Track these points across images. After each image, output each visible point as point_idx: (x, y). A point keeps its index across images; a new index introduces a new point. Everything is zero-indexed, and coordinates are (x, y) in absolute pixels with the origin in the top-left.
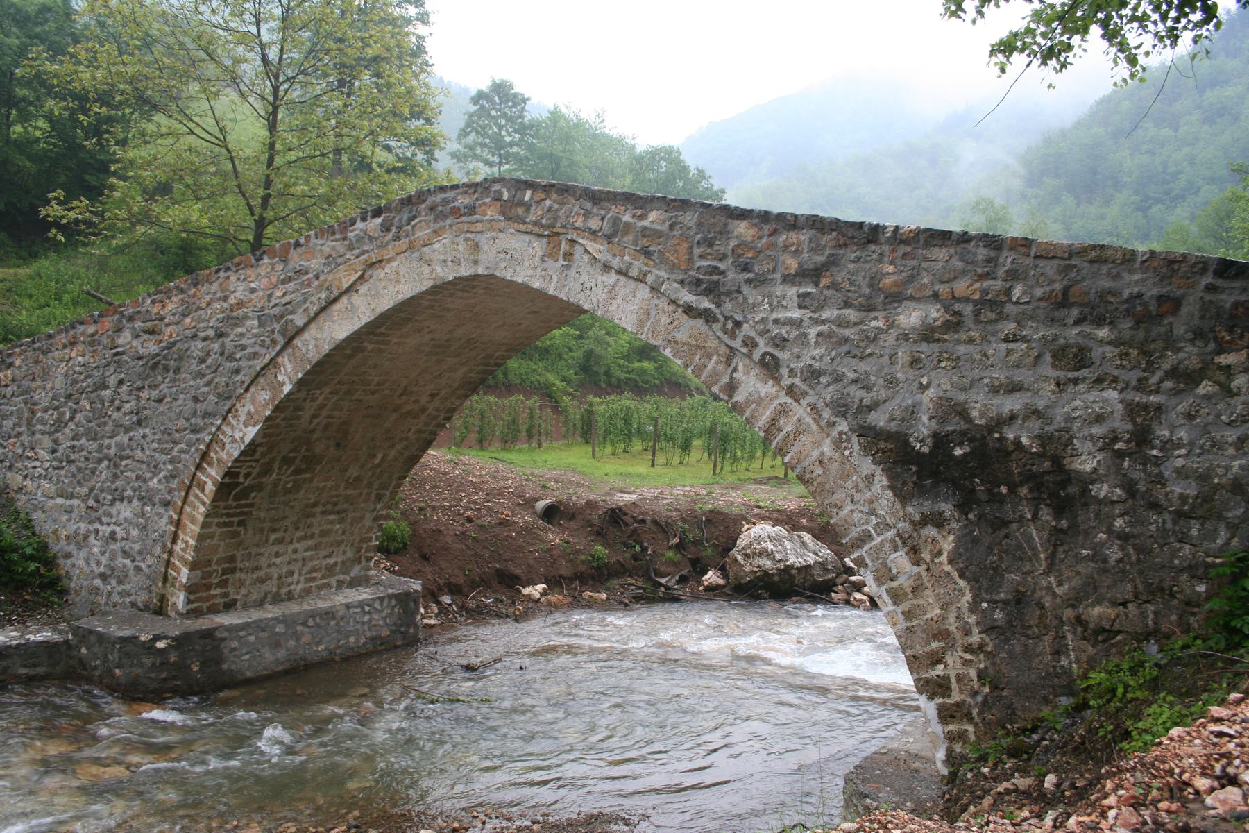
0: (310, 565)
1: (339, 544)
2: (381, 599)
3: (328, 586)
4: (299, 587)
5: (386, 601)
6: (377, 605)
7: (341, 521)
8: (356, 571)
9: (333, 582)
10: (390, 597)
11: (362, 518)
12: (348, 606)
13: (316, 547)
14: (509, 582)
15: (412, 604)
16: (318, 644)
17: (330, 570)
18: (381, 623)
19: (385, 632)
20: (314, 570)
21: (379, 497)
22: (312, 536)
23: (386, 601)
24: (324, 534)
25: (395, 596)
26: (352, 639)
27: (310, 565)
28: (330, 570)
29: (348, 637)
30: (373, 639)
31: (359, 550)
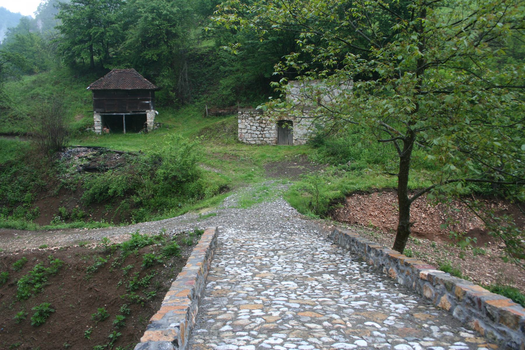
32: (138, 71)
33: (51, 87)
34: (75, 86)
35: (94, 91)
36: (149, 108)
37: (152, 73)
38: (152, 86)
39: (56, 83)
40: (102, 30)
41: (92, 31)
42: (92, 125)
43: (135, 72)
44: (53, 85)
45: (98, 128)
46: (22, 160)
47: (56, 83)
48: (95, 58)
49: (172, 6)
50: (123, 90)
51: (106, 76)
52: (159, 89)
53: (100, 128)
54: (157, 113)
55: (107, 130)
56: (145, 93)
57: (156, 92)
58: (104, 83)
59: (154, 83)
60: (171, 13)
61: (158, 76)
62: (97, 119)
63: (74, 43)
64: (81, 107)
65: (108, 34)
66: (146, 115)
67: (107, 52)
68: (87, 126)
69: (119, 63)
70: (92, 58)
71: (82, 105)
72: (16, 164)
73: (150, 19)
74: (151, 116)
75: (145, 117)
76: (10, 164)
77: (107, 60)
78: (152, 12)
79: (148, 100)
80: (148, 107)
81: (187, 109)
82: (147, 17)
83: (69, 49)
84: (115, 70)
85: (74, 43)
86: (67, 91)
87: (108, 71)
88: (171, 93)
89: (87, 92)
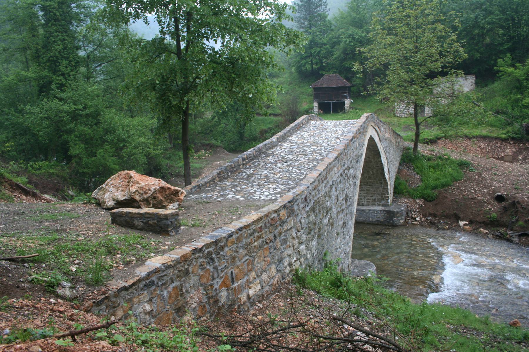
0: (367, 198)
1: (374, 194)
2: (381, 211)
3: (375, 204)
4: (365, 203)
5: (382, 212)
6: (379, 212)
7: (372, 188)
8: (383, 202)
9: (376, 203)
10: (384, 211)
11: (379, 188)
12: (369, 210)
13: (367, 193)
14: (458, 218)
15: (392, 215)
16: (360, 217)
17: (374, 200)
18: (381, 217)
19: (382, 220)
20: (368, 199)
21: (381, 183)
22: (364, 190)
23: (382, 212)
24: (368, 190)
25: (386, 211)
26: (371, 219)
27: (367, 198)
28: (374, 200)
29: (369, 218)
30: (377, 221)
31: (382, 197)
32: (340, 74)
33: (287, 86)
34: (302, 85)
35: (314, 88)
36: (346, 98)
37: (349, 76)
38: (348, 84)
39: (290, 84)
40: (319, 49)
41: (313, 51)
42: (312, 108)
43: (339, 76)
44: (289, 85)
45: (316, 110)
46: (276, 127)
47: (290, 84)
48: (314, 66)
49: (362, 32)
50: (331, 88)
51: (321, 79)
52: (353, 86)
53: (317, 110)
54: (352, 101)
55: (321, 112)
56: (343, 89)
57: (352, 88)
58: (320, 84)
59: (351, 82)
60: (361, 37)
61: (353, 77)
62: (316, 105)
63: (302, 59)
64: (306, 98)
65: (322, 52)
66: (344, 103)
67: (322, 63)
68: (309, 109)
69: (329, 70)
70: (312, 67)
71: (307, 97)
72: (273, 129)
73: (348, 42)
74: (347, 103)
75: (343, 104)
76: (270, 129)
77: (322, 68)
78: (349, 37)
79: (346, 93)
80: (346, 97)
81: (372, 98)
82: (346, 41)
83: (299, 62)
84: (327, 75)
85: (302, 59)
86: (297, 88)
87: (322, 75)
88: (361, 88)
89: (310, 89)
